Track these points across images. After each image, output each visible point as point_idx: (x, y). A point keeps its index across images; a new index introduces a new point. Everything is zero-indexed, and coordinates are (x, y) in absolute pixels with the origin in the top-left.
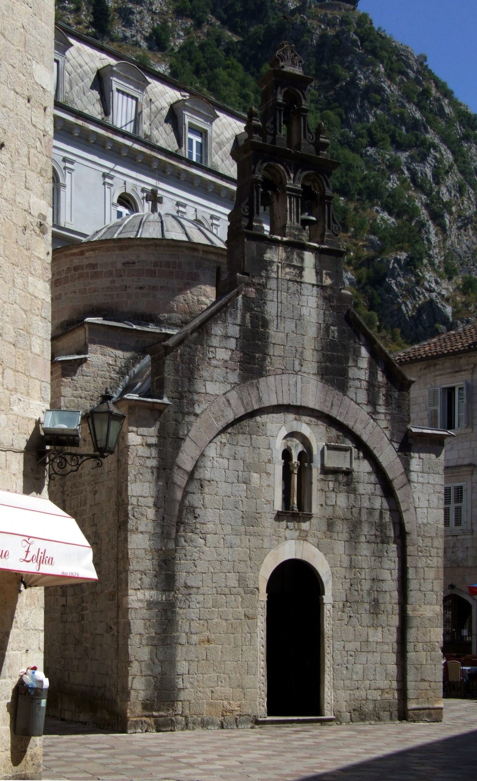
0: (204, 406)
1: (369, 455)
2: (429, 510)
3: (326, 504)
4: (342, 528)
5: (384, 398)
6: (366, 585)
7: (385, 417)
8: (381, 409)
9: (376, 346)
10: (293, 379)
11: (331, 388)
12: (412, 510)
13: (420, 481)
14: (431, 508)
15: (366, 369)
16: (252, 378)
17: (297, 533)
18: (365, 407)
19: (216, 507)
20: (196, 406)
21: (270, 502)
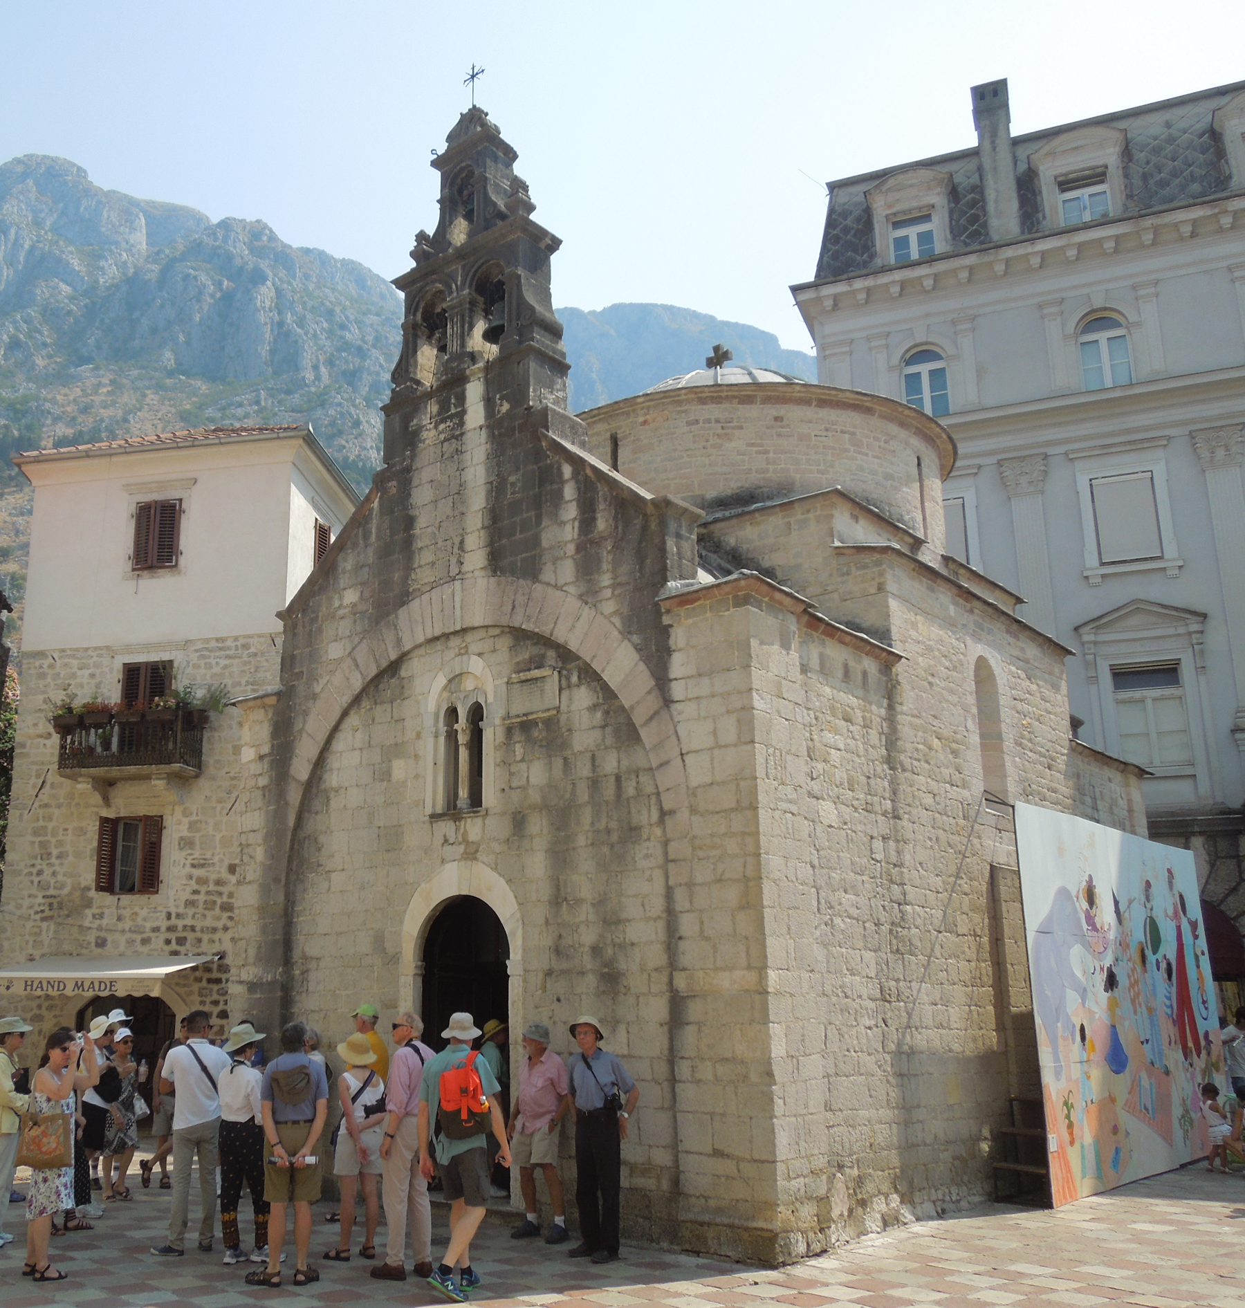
0: (323, 681)
1: (590, 675)
2: (716, 752)
3: (511, 788)
4: (538, 826)
5: (610, 558)
8: (606, 580)
9: (588, 471)
10: (447, 589)
11: (510, 579)
13: (690, 696)
14: (720, 747)
16: (388, 615)
17: (462, 848)
18: (571, 589)
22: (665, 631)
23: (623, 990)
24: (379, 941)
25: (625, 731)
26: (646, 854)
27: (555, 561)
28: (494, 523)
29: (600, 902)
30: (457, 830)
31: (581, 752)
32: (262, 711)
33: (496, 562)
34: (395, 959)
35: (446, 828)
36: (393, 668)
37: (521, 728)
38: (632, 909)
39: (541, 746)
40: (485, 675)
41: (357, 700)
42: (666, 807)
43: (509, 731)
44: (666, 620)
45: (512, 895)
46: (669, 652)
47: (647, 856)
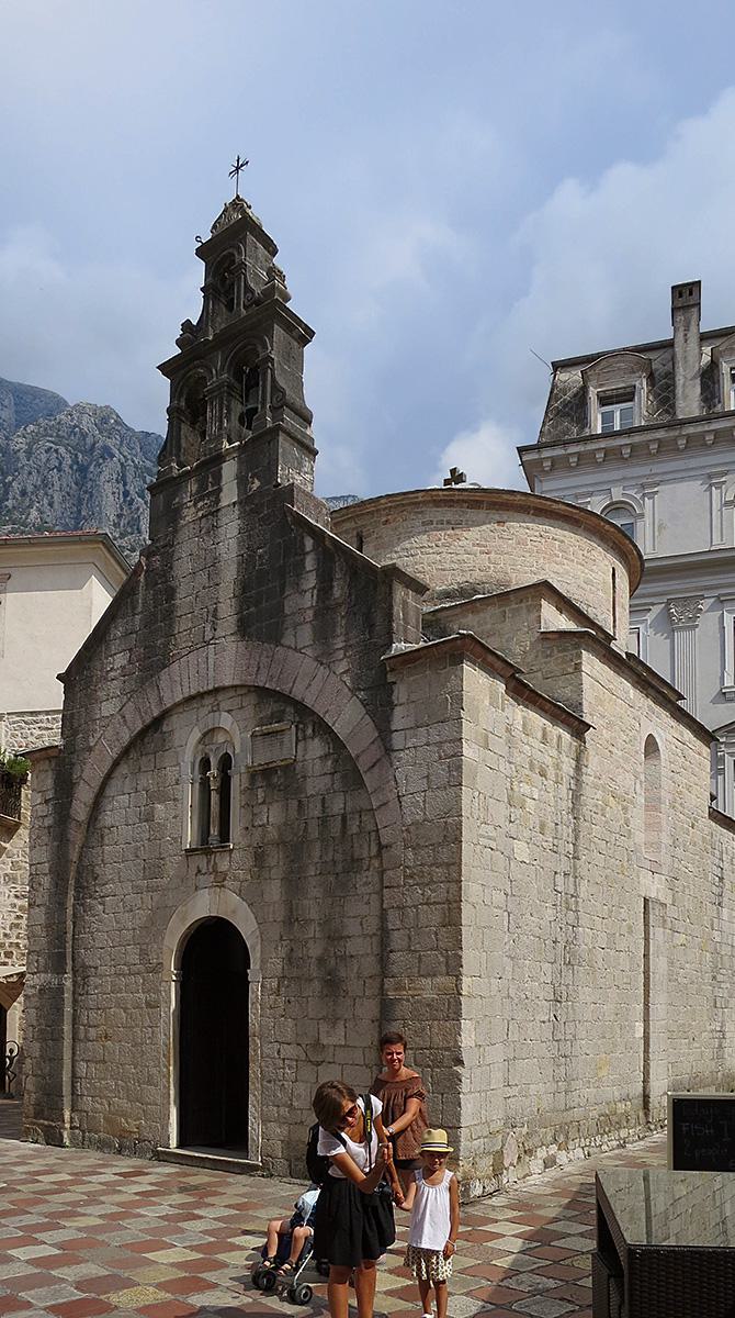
1: (323, 729)
4: (275, 859)
6: (315, 950)
7: (346, 651)
12: (394, 804)
15: (314, 587)
19: (116, 860)
20: (91, 739)
21: (178, 839)
22: (388, 688)
23: (342, 994)
24: (143, 954)
25: (348, 773)
26: (365, 881)
27: (296, 626)
28: (244, 592)
29: (325, 922)
30: (208, 863)
31: (312, 796)
32: (47, 762)
33: (244, 629)
34: (158, 968)
35: (201, 861)
36: (157, 722)
37: (263, 775)
38: (352, 928)
39: (279, 790)
40: (235, 728)
41: (126, 752)
42: (384, 842)
43: (253, 776)
44: (390, 678)
45: (252, 916)
46: (391, 706)
47: (366, 884)
